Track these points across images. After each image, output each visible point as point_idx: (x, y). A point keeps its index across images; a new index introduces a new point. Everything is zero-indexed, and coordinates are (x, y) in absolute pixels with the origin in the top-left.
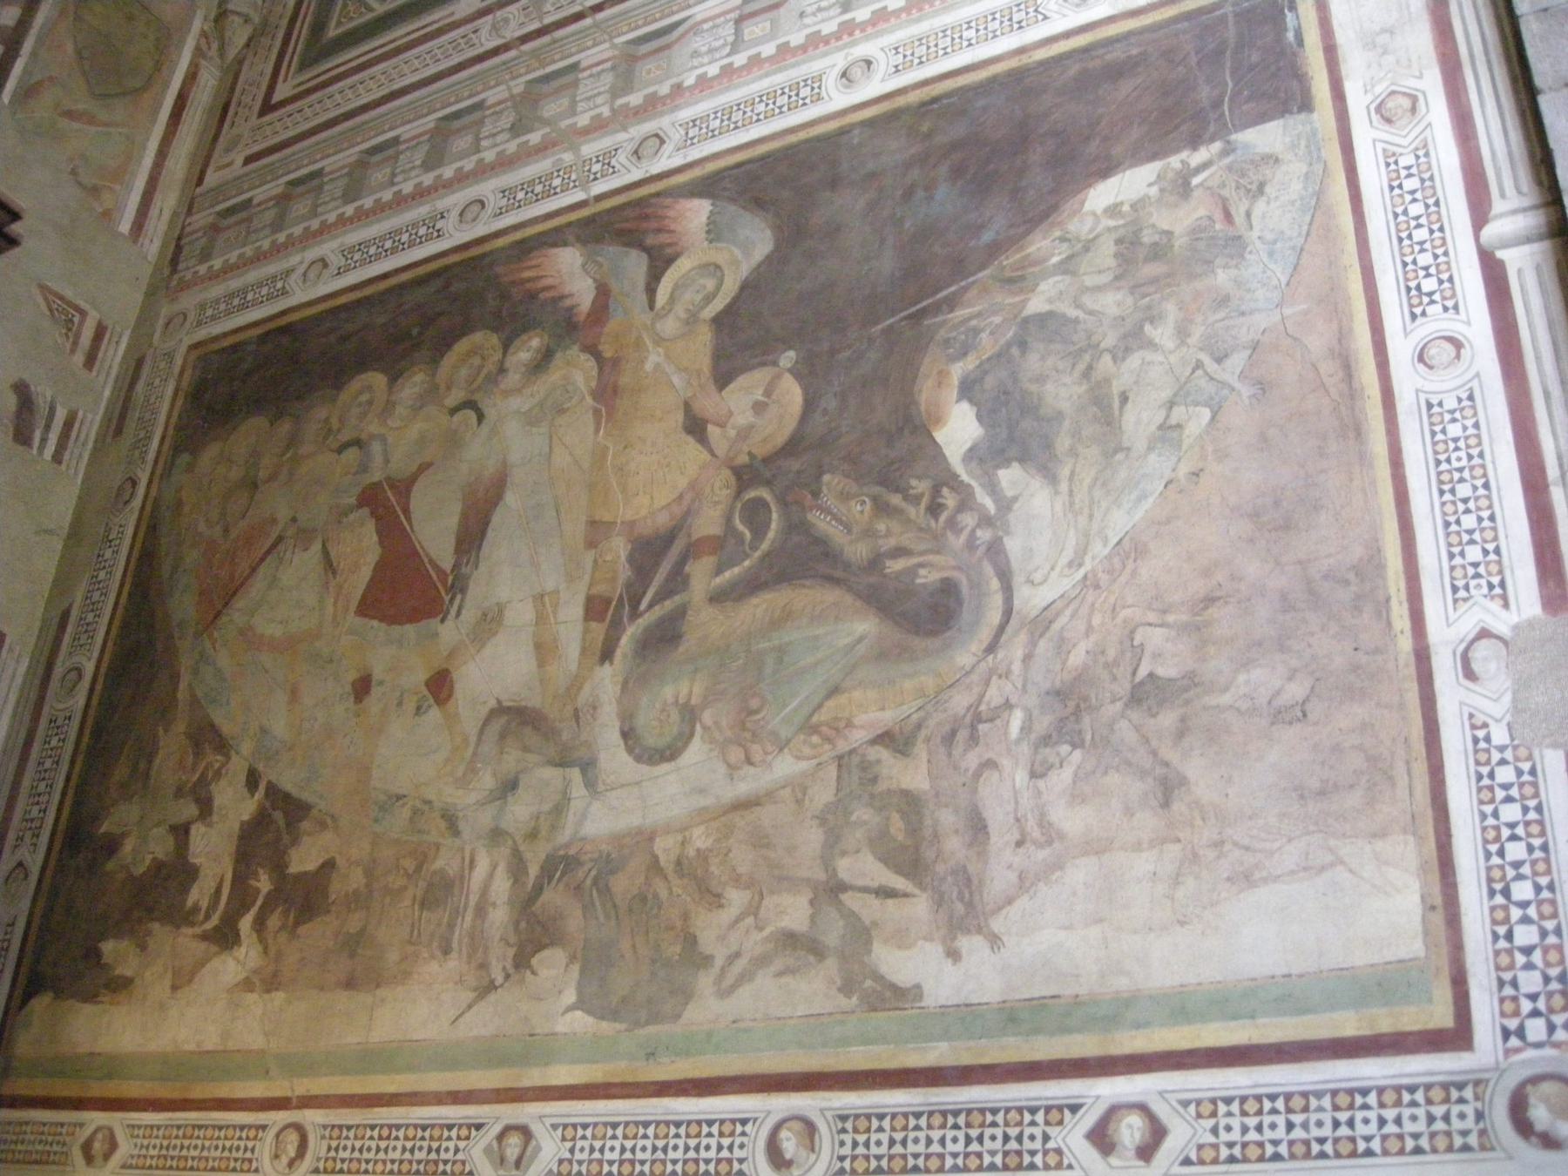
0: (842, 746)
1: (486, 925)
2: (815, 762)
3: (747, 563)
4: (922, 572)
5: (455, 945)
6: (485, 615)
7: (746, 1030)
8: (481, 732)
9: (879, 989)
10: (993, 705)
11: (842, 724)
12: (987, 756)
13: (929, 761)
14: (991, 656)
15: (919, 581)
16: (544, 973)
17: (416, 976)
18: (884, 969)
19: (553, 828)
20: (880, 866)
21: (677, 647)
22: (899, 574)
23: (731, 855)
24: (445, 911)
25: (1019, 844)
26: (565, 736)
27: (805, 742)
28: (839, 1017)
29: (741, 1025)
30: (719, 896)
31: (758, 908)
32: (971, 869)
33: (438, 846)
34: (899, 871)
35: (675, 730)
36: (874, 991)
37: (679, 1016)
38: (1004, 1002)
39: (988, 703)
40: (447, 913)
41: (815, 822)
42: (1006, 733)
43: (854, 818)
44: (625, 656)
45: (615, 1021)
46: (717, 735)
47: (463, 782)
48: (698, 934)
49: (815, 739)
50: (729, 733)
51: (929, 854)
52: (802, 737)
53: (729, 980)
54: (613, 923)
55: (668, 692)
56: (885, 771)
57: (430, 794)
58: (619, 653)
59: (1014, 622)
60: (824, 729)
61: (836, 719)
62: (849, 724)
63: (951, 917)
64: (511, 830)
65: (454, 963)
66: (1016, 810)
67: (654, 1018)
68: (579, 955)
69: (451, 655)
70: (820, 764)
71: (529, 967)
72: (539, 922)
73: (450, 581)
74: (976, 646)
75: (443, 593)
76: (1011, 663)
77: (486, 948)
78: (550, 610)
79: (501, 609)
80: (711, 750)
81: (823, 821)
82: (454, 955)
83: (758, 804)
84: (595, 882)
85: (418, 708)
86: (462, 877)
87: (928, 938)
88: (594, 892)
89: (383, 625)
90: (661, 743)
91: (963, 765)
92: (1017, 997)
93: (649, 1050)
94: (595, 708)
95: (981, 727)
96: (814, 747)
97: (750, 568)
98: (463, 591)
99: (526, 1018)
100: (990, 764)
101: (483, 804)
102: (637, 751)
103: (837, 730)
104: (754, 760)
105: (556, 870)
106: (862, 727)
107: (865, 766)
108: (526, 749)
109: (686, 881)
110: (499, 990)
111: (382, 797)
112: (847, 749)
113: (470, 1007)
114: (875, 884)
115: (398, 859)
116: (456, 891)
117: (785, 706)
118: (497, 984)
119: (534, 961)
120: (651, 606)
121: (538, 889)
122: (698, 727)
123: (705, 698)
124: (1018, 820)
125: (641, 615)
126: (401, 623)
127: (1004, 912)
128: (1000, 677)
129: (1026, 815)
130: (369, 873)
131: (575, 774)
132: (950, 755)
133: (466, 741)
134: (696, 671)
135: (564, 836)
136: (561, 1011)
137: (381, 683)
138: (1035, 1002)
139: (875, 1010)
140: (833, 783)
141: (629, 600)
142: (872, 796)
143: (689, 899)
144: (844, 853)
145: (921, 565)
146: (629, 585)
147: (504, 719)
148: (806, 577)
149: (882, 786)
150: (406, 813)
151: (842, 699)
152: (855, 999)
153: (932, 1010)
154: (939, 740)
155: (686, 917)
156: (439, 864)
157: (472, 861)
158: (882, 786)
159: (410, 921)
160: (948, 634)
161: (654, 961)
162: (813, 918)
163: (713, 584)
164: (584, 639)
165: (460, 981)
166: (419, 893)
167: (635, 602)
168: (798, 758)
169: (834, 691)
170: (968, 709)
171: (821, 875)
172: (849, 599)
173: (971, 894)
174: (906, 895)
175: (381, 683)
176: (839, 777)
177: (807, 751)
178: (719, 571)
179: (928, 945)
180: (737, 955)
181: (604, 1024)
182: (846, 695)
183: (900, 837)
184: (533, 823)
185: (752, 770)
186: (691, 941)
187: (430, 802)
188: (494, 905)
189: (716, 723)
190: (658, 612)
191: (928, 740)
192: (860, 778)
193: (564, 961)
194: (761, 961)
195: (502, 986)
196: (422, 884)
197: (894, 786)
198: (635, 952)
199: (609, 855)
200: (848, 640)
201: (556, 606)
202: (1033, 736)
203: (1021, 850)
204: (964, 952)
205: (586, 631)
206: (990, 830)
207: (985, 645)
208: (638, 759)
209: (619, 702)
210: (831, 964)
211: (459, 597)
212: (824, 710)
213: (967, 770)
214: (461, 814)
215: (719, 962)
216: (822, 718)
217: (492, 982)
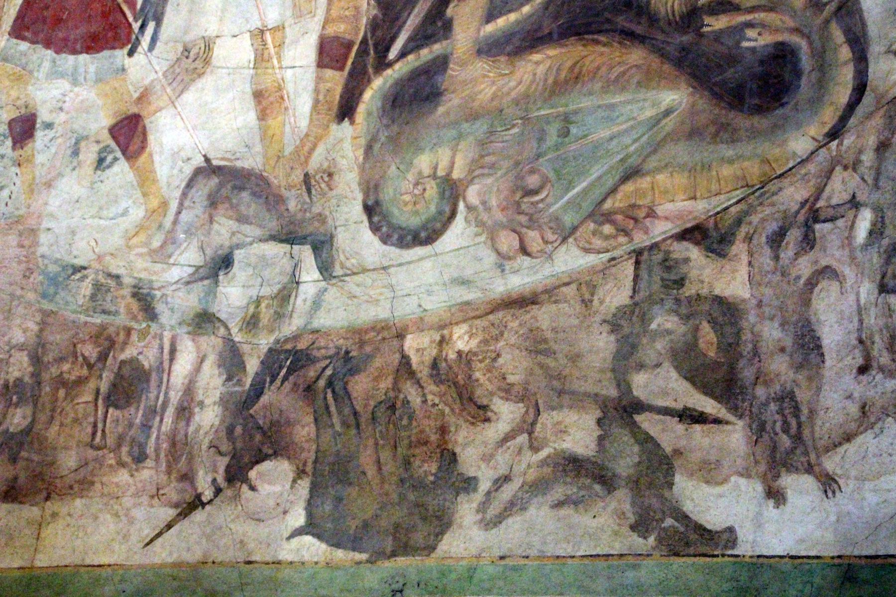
0: (641, 240)
1: (191, 429)
2: (606, 256)
3: (526, 9)
4: (751, 33)
5: (150, 449)
6: (186, 50)
7: (515, 569)
8: (184, 195)
9: (682, 529)
10: (834, 201)
11: (641, 214)
12: (824, 263)
13: (750, 263)
14: (835, 143)
15: (745, 44)
16: (265, 489)
17: (98, 486)
18: (688, 507)
19: (279, 316)
20: (687, 385)
21: (436, 107)
22: (718, 36)
23: (501, 361)
24: (138, 409)
25: (863, 370)
26: (292, 205)
27: (594, 233)
28: (631, 560)
29: (507, 561)
30: (484, 408)
31: (534, 424)
32: (803, 395)
33: (128, 331)
34: (707, 390)
35: (433, 209)
36: (676, 532)
37: (433, 548)
38: (840, 557)
39: (829, 198)
40: (141, 412)
41: (606, 328)
42: (850, 238)
43: (653, 326)
44: (369, 114)
45: (354, 550)
46: (484, 216)
47: (161, 255)
48: (458, 450)
49: (607, 229)
50: (499, 216)
51: (747, 374)
52: (592, 226)
53: (493, 510)
54: (353, 431)
55: (423, 162)
56: (693, 274)
57: (116, 266)
58: (361, 110)
59: (868, 99)
60: (619, 217)
61: (633, 206)
62: (651, 214)
63: (774, 449)
64: (223, 316)
65: (147, 474)
66: (860, 330)
67: (404, 548)
68: (309, 468)
69: (143, 97)
70: (613, 259)
71: (246, 480)
72: (260, 428)
73: (139, 6)
74: (816, 129)
75: (131, 19)
76: (860, 152)
77: (190, 460)
78: (272, 51)
79: (208, 45)
80: (477, 235)
81: (614, 326)
82: (149, 463)
83: (534, 303)
84: (330, 384)
85: (101, 161)
86: (160, 369)
87: (746, 474)
88: (330, 396)
89: (50, 53)
90: (414, 222)
91: (794, 273)
92: (856, 553)
93: (396, 587)
94: (330, 175)
95: (818, 226)
96: (607, 238)
97: (531, 16)
98: (159, 20)
99: (241, 542)
100: (827, 272)
101: (188, 283)
102: (384, 229)
103: (636, 220)
104: (529, 250)
105: (281, 368)
106: (667, 218)
107: (668, 264)
108: (242, 219)
109: (443, 388)
110: (208, 507)
111: (53, 269)
112: (648, 243)
113: (169, 526)
114: (679, 406)
115: (75, 346)
116: (153, 383)
117: (568, 190)
118: (205, 499)
119: (252, 474)
120: (403, 55)
121: (257, 391)
122: (461, 206)
123: (471, 171)
124: (861, 342)
125: (390, 65)
126: (74, 52)
127: (841, 450)
128: (846, 168)
129: (871, 337)
130: (36, 360)
131: (306, 253)
132: (777, 258)
133: (165, 204)
134: (460, 137)
135: (289, 328)
136: (286, 534)
137: (49, 126)
138: (879, 561)
139: (677, 554)
140: (629, 283)
141: (376, 46)
142: (677, 301)
143: (447, 410)
144: (641, 366)
145: (750, 25)
146: (374, 25)
147: (214, 181)
148: (599, 32)
149: (689, 290)
150: (86, 288)
151: (644, 183)
152: (652, 540)
153: (747, 559)
154: (764, 239)
155: (443, 430)
156: (129, 353)
157: (173, 351)
158: (689, 290)
159: (91, 419)
160: (780, 112)
161: (402, 481)
162: (601, 439)
163: (482, 33)
164: (317, 91)
165: (157, 494)
166: (104, 387)
167: (383, 48)
168: (587, 251)
169: (631, 174)
170: (803, 204)
171: (613, 392)
172: (655, 61)
173: (799, 425)
174: (717, 421)
175: (49, 126)
176: (636, 278)
177: (598, 243)
178: (490, 17)
179: (742, 481)
180: (507, 479)
181: (340, 554)
182: (648, 179)
183: (712, 354)
184: (252, 309)
185: (526, 261)
186: (449, 458)
187: (118, 277)
188: (201, 404)
189: (484, 203)
190: (412, 61)
191: (749, 239)
192: (662, 279)
193: (291, 475)
194: (538, 487)
195: (210, 502)
196: (107, 377)
197: (704, 292)
198: (380, 469)
199: (347, 352)
200: (649, 113)
201: (280, 46)
202: (885, 242)
203: (864, 378)
204: (790, 494)
205: (319, 79)
206: (826, 350)
207: (826, 129)
208: (385, 240)
209: (362, 169)
210: (622, 499)
211: (151, 26)
212: (619, 196)
213: (798, 277)
214: (158, 294)
215: (484, 486)
216: (617, 205)
217: (198, 496)
